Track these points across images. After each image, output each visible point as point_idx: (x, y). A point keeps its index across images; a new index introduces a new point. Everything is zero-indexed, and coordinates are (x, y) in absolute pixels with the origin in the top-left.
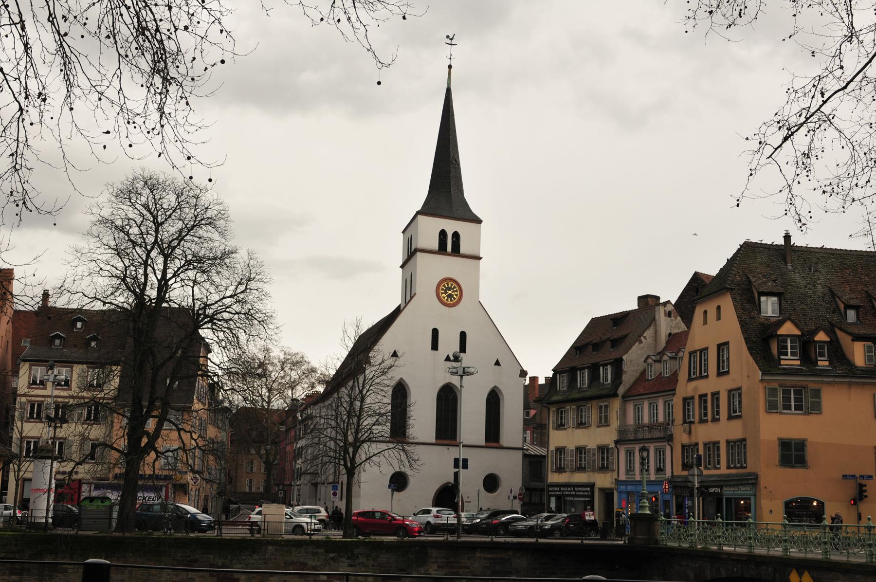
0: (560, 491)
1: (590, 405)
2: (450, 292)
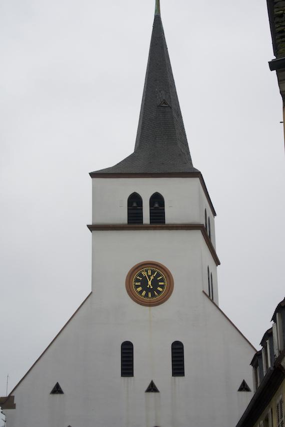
2: (150, 283)
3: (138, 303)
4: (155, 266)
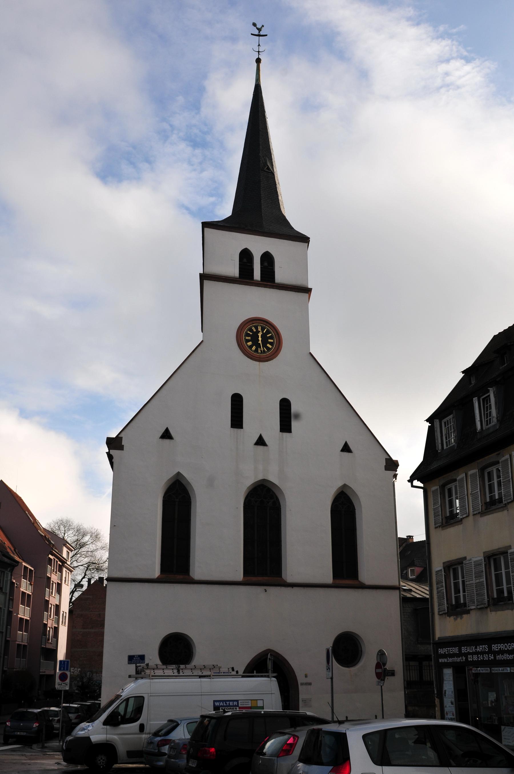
0: (460, 654)
1: (507, 456)
2: (260, 339)
3: (249, 357)
4: (265, 323)
